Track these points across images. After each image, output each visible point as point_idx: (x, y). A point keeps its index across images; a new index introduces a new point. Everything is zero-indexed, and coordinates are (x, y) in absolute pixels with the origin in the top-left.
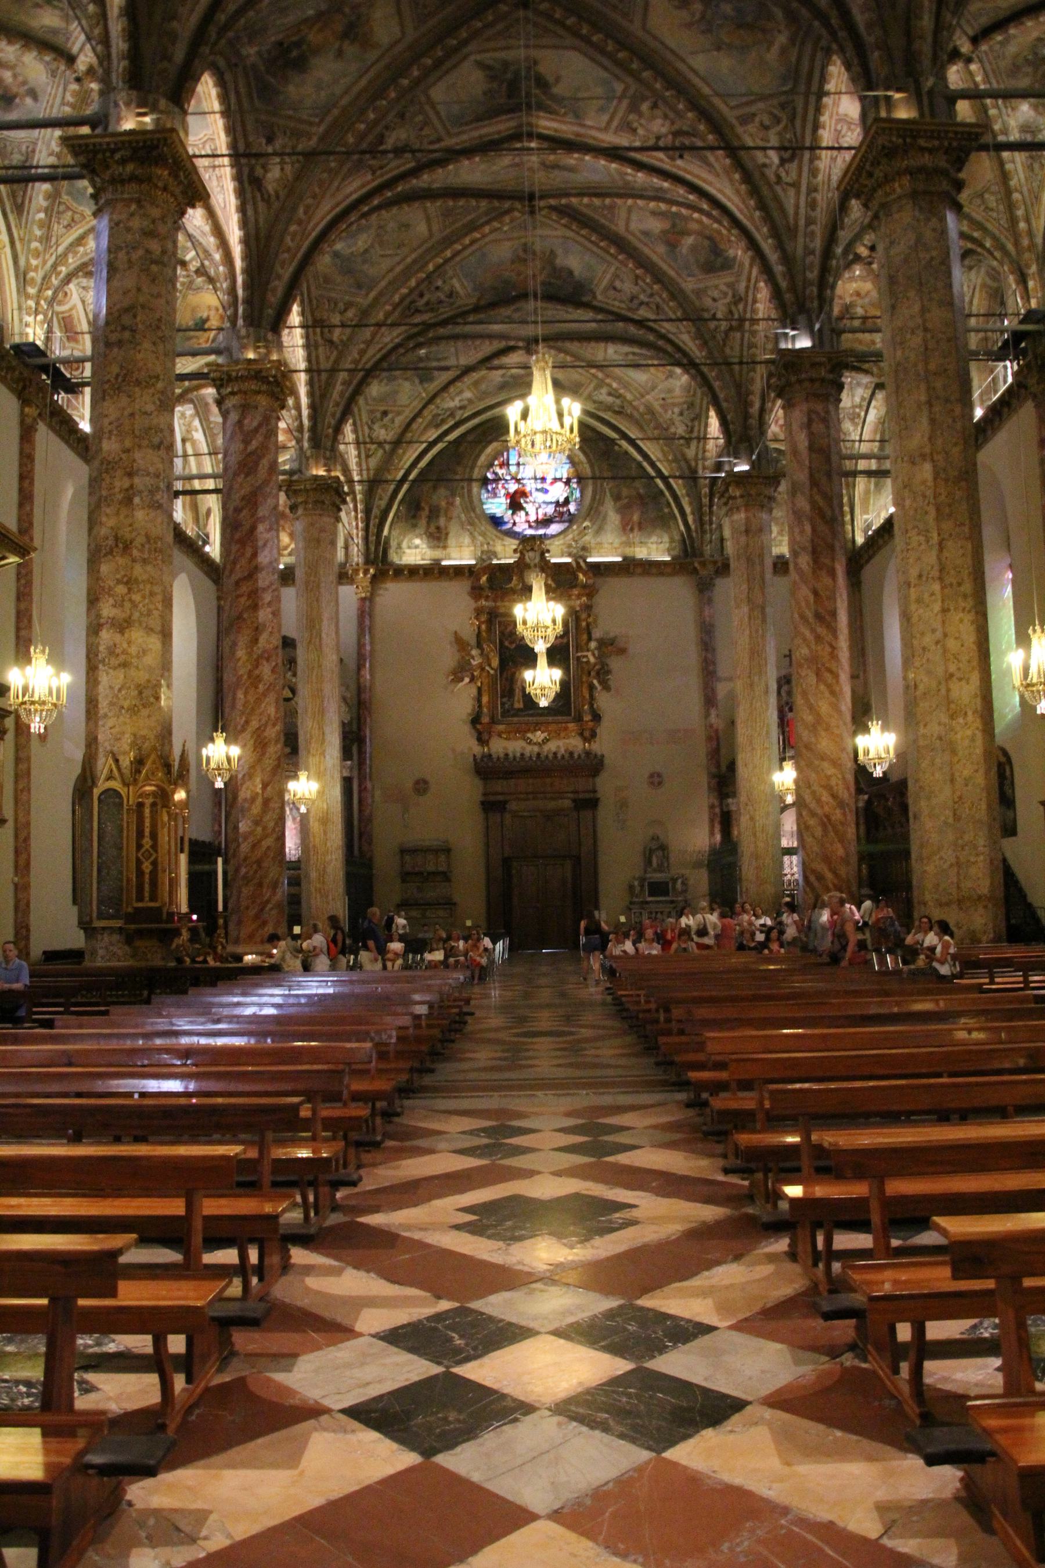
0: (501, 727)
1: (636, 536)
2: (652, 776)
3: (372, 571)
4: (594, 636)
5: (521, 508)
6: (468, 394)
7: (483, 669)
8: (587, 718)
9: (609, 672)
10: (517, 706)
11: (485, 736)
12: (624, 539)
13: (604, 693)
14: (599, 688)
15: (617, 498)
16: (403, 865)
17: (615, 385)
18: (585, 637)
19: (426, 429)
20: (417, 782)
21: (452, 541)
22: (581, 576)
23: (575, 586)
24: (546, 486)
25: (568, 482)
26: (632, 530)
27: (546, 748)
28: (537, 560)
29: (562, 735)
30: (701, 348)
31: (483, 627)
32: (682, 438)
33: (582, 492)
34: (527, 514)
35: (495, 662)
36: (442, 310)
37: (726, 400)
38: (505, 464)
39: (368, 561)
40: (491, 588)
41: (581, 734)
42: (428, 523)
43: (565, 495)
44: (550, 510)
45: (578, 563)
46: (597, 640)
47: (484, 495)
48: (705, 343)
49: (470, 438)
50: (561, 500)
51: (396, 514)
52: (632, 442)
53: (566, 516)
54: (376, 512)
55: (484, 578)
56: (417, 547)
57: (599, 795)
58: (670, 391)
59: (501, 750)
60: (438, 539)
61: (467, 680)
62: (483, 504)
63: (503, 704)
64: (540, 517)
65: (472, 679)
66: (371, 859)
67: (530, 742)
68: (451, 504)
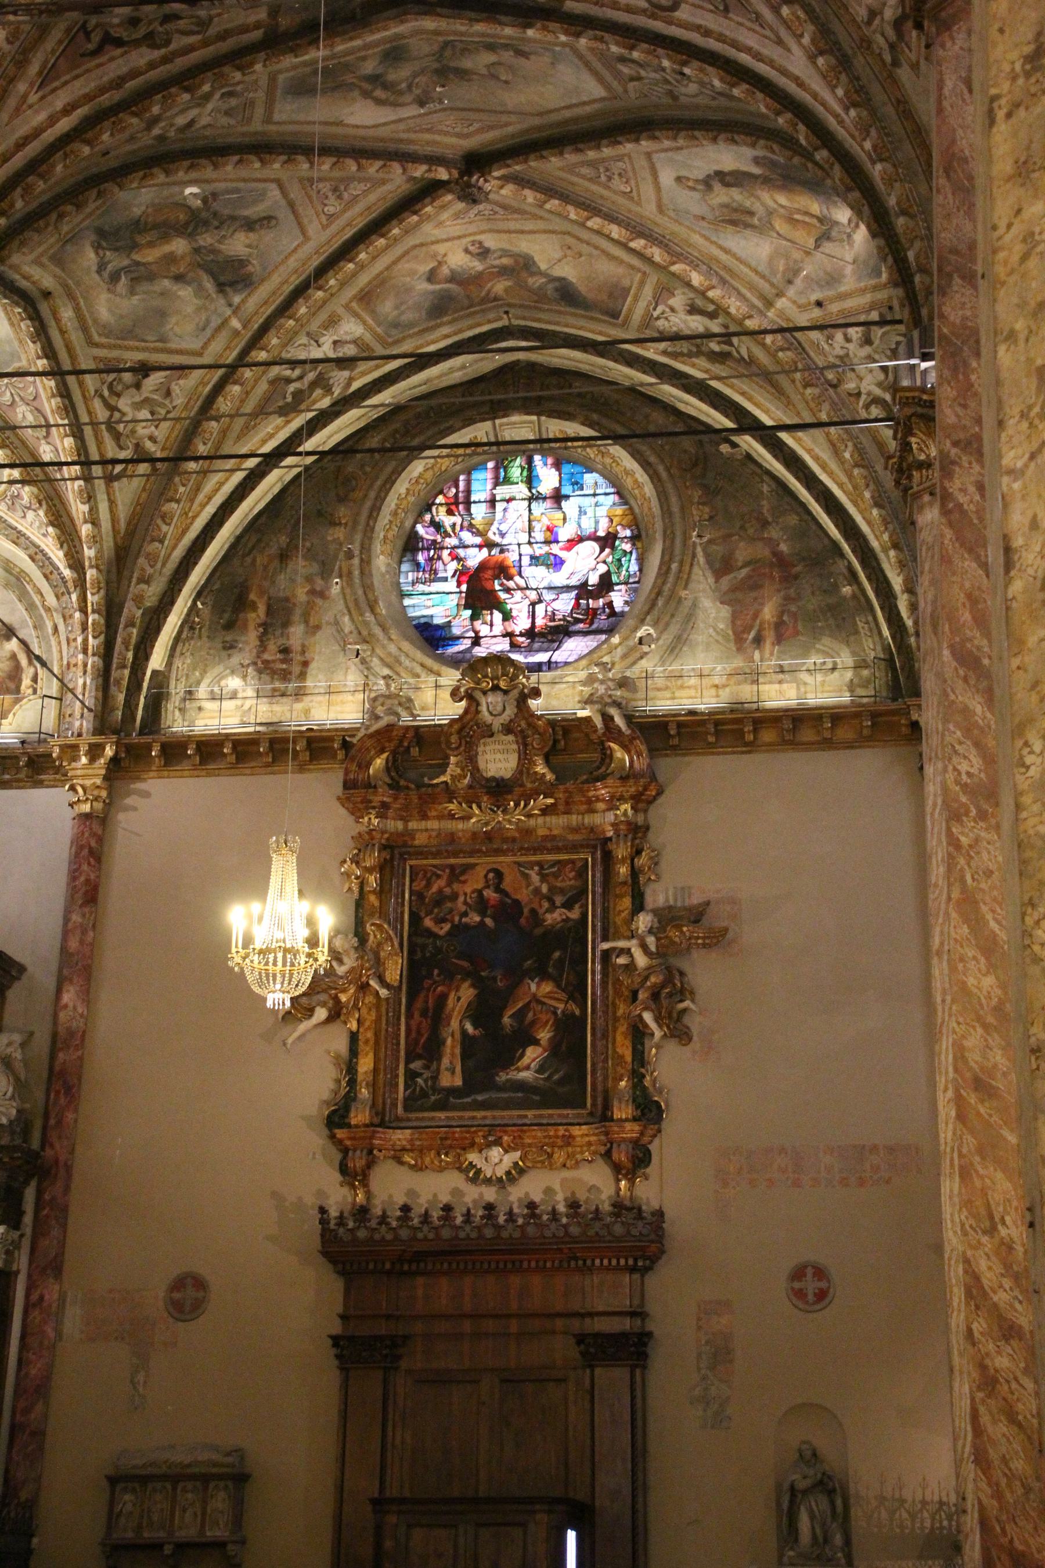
0: (401, 1137)
1: (768, 658)
2: (798, 1274)
3: (109, 751)
4: (650, 901)
5: (497, 604)
6: (351, 328)
7: (364, 987)
8: (622, 1111)
9: (684, 992)
10: (446, 1080)
11: (358, 1161)
12: (738, 662)
13: (672, 1047)
14: (658, 1034)
15: (722, 567)
16: (112, 1518)
17: (696, 279)
18: (627, 902)
19: (261, 412)
20: (179, 1284)
21: (315, 681)
22: (619, 753)
23: (602, 778)
24: (555, 549)
25: (607, 541)
26: (758, 641)
27: (516, 1193)
28: (510, 712)
29: (559, 1156)
30: (830, 80)
31: (373, 880)
32: (876, 401)
33: (641, 561)
34: (507, 617)
35: (395, 970)
36: (179, 42)
37: (904, 213)
38: (462, 503)
39: (102, 726)
40: (394, 786)
41: (607, 1155)
42: (263, 639)
43: (603, 569)
44: (564, 604)
45: (607, 719)
46: (655, 912)
47: (408, 576)
48: (844, 63)
49: (374, 441)
50: (594, 579)
51: (188, 623)
52: (767, 436)
53: (601, 622)
54: (132, 611)
55: (379, 762)
56: (234, 696)
57: (650, 1326)
58: (832, 279)
59: (400, 1199)
60: (285, 676)
61: (321, 1014)
62: (402, 595)
63: (411, 1076)
64: (540, 622)
65: (336, 1014)
66: (31, 1504)
67: (476, 1177)
68: (322, 595)
